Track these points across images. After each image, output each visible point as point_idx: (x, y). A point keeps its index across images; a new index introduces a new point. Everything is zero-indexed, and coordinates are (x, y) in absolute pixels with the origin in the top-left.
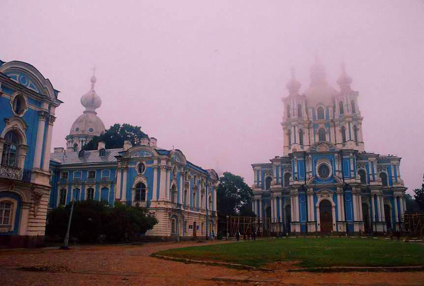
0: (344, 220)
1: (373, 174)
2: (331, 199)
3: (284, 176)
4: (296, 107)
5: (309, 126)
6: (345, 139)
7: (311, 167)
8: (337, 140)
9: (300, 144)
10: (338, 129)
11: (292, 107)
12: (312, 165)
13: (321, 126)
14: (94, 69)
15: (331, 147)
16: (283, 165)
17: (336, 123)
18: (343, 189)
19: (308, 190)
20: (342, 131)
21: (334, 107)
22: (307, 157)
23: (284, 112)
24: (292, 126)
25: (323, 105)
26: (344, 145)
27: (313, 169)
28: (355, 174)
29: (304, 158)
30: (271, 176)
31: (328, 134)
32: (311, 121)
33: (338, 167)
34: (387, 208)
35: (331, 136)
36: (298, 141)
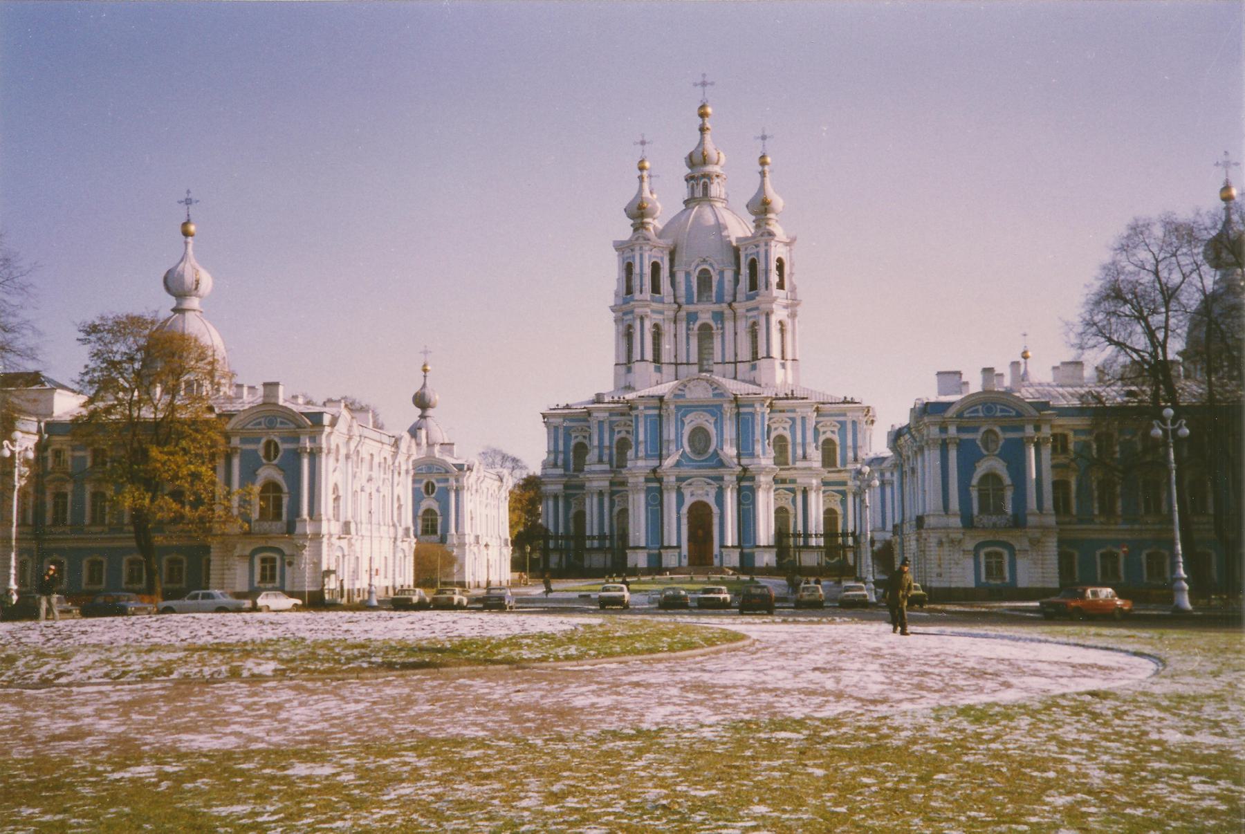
0: (736, 544)
1: (804, 445)
2: (711, 501)
3: (614, 442)
4: (648, 270)
5: (676, 317)
6: (757, 353)
7: (673, 430)
8: (739, 354)
9: (655, 361)
10: (743, 326)
11: (637, 270)
12: (677, 429)
13: (705, 318)
14: (188, 202)
16: (614, 418)
19: (665, 479)
22: (664, 407)
23: (618, 279)
24: (634, 319)
25: (711, 265)
26: (754, 368)
27: (677, 434)
29: (660, 408)
30: (586, 442)
33: (730, 431)
34: (830, 515)
35: (727, 342)
36: (649, 355)
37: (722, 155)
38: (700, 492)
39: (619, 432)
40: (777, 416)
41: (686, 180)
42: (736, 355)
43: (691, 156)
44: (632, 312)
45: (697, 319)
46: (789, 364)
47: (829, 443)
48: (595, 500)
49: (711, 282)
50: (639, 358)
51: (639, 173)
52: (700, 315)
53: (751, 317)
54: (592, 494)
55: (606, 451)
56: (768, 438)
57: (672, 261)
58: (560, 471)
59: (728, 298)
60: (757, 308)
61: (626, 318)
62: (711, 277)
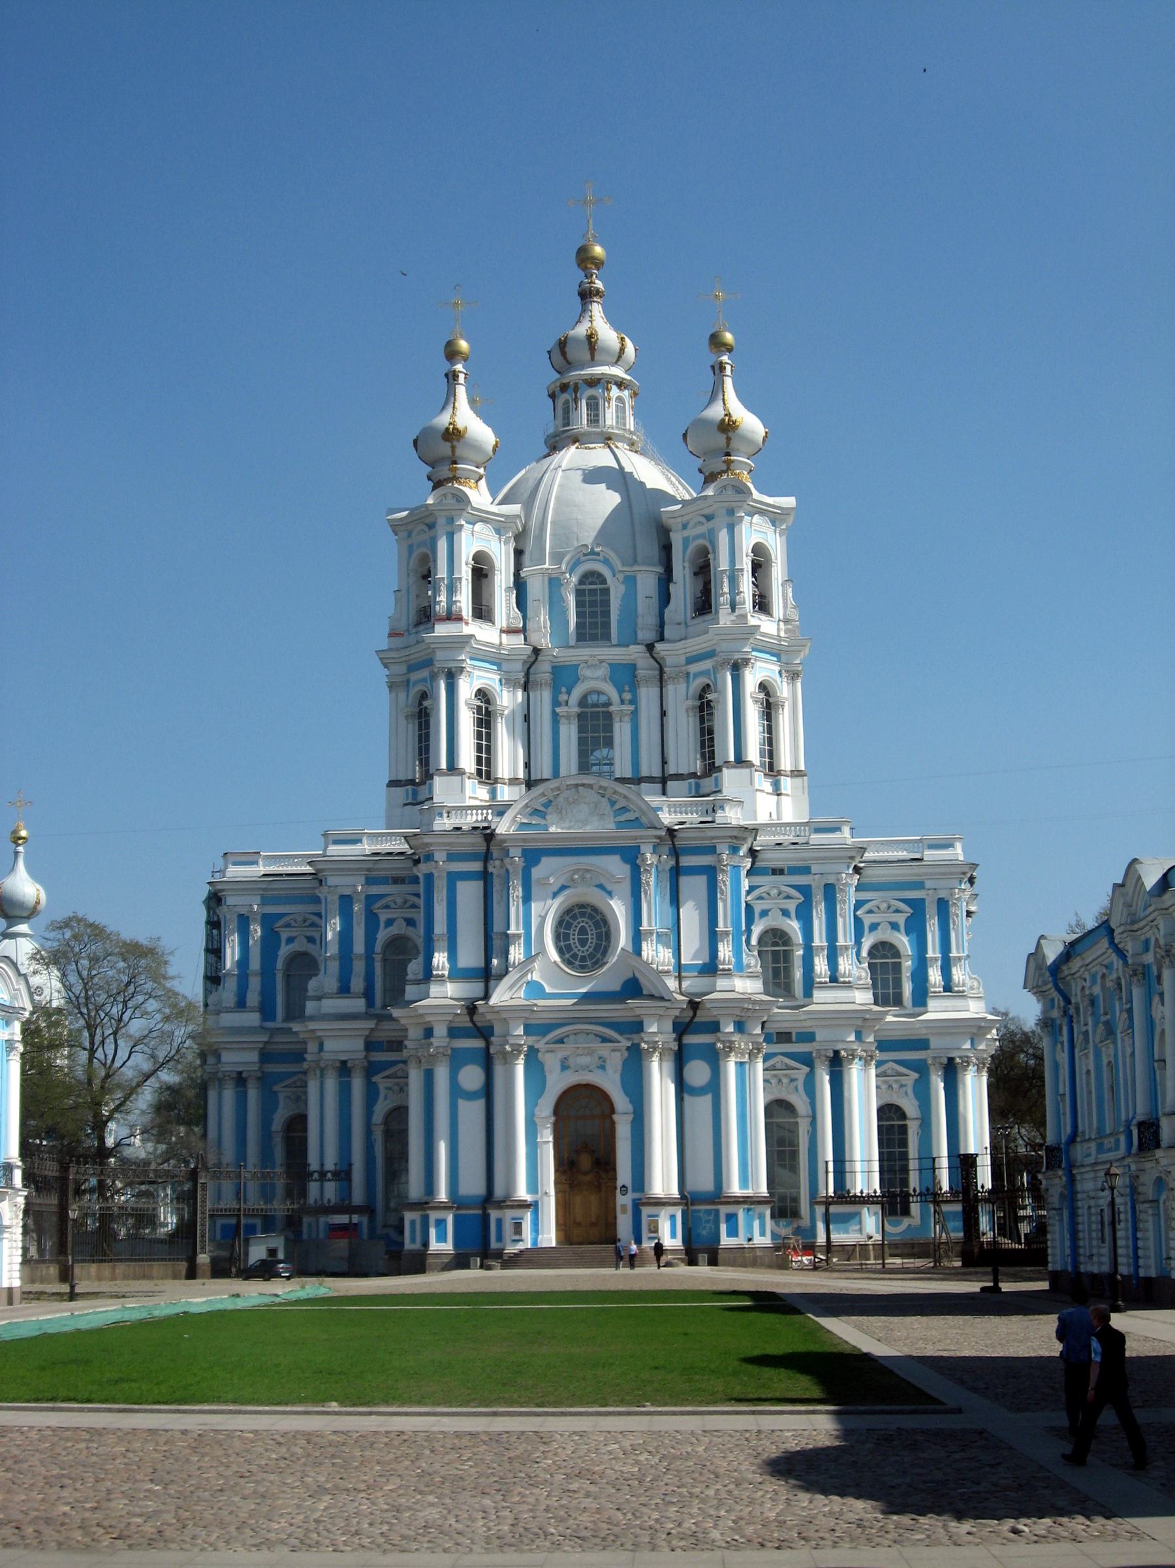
2: (611, 1083)
3: (378, 948)
4: (465, 573)
5: (527, 674)
6: (712, 754)
10: (680, 697)
15: (624, 809)
17: (669, 661)
18: (676, 1025)
19: (497, 1030)
20: (701, 708)
21: (666, 578)
22: (495, 853)
24: (434, 677)
25: (606, 562)
28: (738, 953)
29: (486, 857)
31: (627, 719)
32: (536, 651)
34: (890, 1116)
36: (467, 759)
37: (629, 344)
38: (584, 1060)
39: (390, 922)
40: (766, 881)
41: (553, 396)
42: (664, 762)
43: (562, 344)
44: (428, 663)
45: (577, 680)
46: (786, 783)
47: (883, 950)
48: (331, 1084)
49: (606, 603)
50: (443, 765)
51: (445, 366)
52: (584, 672)
53: (698, 675)
54: (322, 1071)
55: (359, 967)
56: (749, 931)
57: (519, 553)
58: (252, 1019)
59: (646, 635)
60: (710, 654)
61: (415, 676)
62: (606, 592)
